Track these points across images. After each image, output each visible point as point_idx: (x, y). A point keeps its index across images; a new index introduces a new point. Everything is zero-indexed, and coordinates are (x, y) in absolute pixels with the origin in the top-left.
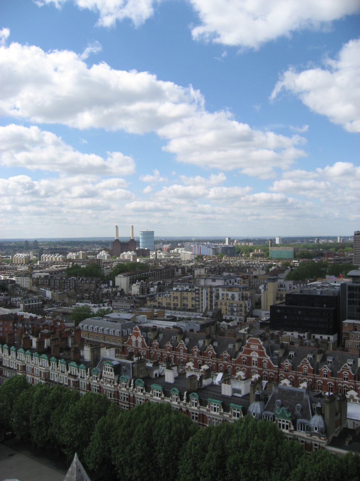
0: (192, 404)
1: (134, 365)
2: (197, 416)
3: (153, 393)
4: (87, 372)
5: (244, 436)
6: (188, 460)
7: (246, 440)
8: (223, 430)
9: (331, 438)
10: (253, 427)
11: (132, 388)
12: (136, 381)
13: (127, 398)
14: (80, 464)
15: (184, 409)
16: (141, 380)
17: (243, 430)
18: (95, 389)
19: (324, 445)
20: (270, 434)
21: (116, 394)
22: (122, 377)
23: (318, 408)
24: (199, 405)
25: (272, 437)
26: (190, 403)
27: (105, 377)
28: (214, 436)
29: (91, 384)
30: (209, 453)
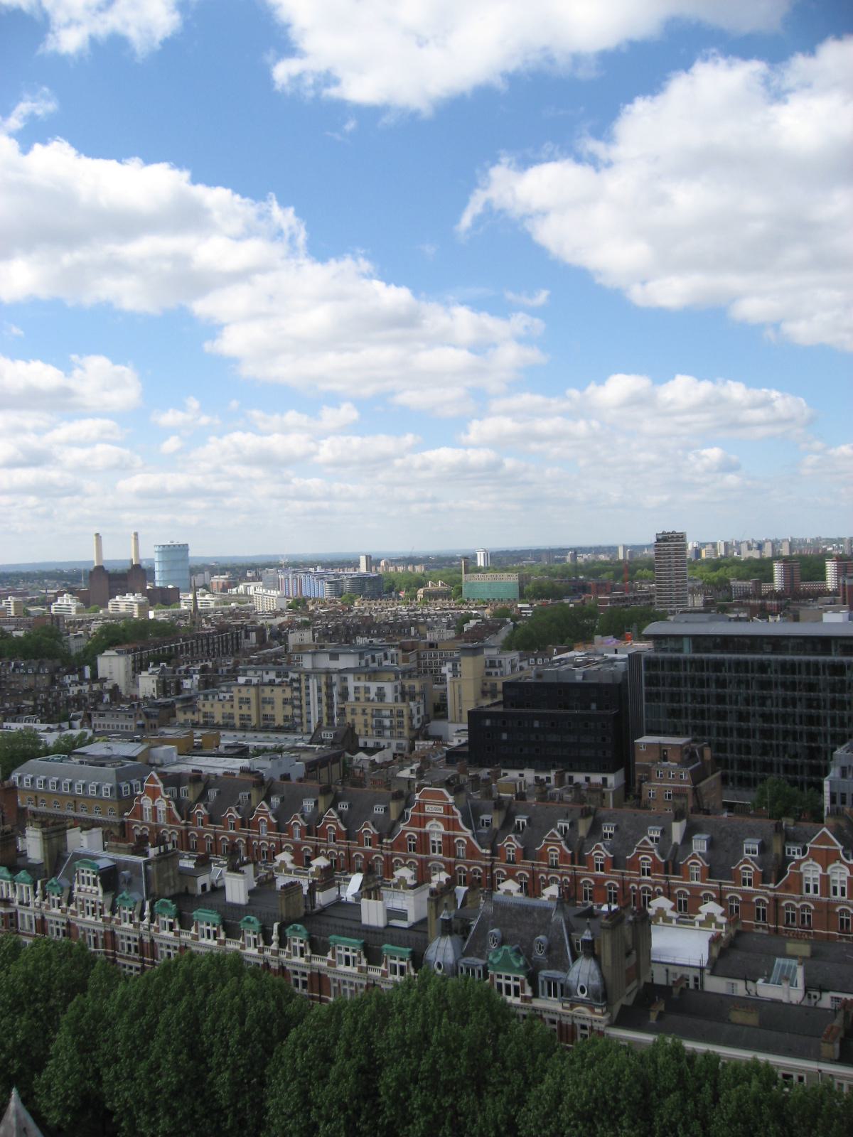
0: (292, 951)
1: (150, 867)
2: (306, 979)
3: (199, 931)
4: (35, 889)
5: (418, 1019)
6: (288, 1085)
7: (423, 1027)
8: (368, 1007)
9: (616, 1008)
11: (146, 921)
12: (156, 906)
13: (136, 947)
14: (25, 1114)
15: (274, 965)
16: (169, 901)
17: (414, 1006)
18: (58, 930)
19: (601, 1026)
20: (478, 1010)
21: (109, 938)
22: (121, 896)
23: (585, 941)
24: (308, 954)
25: (483, 1016)
26: (287, 950)
27: (80, 900)
28: (347, 1022)
29: (47, 917)
30: (338, 1064)
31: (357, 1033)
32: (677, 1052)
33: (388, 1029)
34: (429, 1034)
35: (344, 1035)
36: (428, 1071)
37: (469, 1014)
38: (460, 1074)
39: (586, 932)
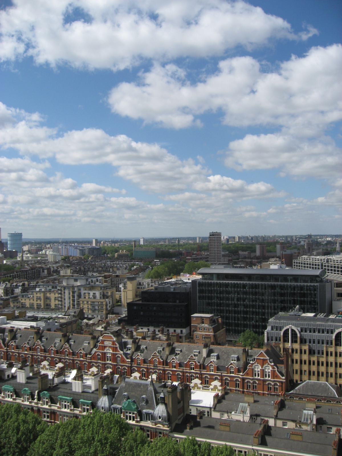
2: (49, 414)
3: (5, 394)
7: (92, 434)
8: (70, 426)
9: (174, 425)
10: (99, 421)
17: (89, 425)
20: (115, 426)
23: (161, 397)
25: (117, 429)
26: (41, 402)
30: (57, 451)
31: (65, 437)
32: (194, 443)
33: (78, 435)
34: (94, 437)
35: (60, 438)
36: (93, 453)
37: (111, 428)
38: (106, 453)
39: (162, 394)
